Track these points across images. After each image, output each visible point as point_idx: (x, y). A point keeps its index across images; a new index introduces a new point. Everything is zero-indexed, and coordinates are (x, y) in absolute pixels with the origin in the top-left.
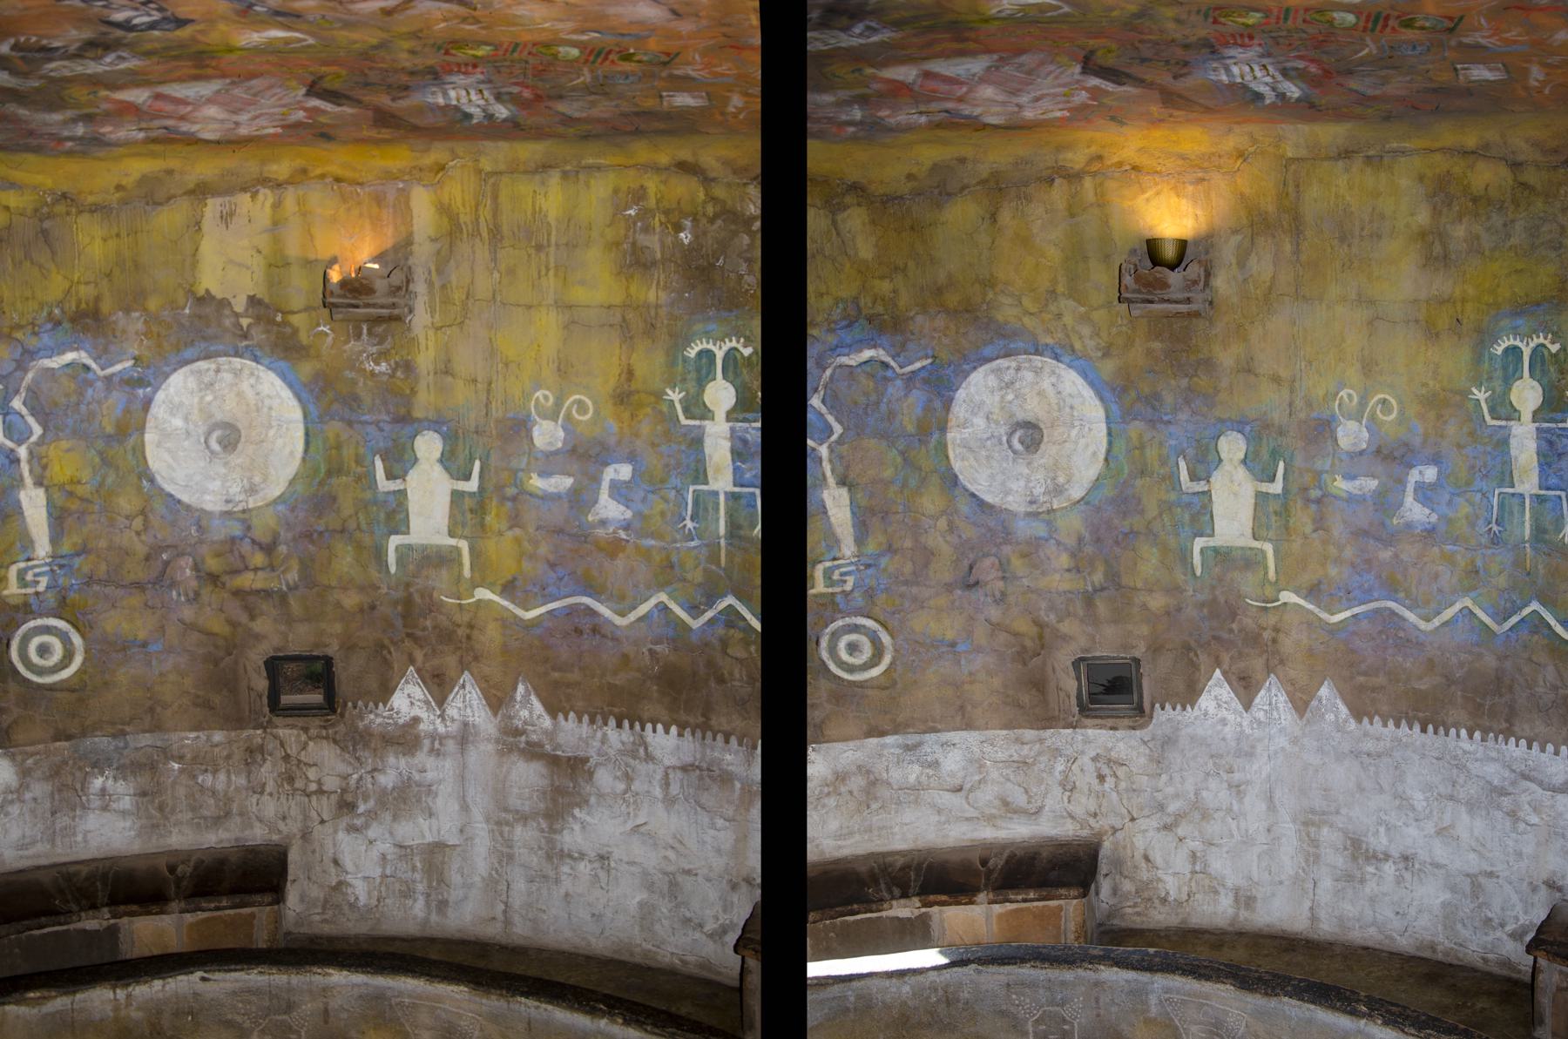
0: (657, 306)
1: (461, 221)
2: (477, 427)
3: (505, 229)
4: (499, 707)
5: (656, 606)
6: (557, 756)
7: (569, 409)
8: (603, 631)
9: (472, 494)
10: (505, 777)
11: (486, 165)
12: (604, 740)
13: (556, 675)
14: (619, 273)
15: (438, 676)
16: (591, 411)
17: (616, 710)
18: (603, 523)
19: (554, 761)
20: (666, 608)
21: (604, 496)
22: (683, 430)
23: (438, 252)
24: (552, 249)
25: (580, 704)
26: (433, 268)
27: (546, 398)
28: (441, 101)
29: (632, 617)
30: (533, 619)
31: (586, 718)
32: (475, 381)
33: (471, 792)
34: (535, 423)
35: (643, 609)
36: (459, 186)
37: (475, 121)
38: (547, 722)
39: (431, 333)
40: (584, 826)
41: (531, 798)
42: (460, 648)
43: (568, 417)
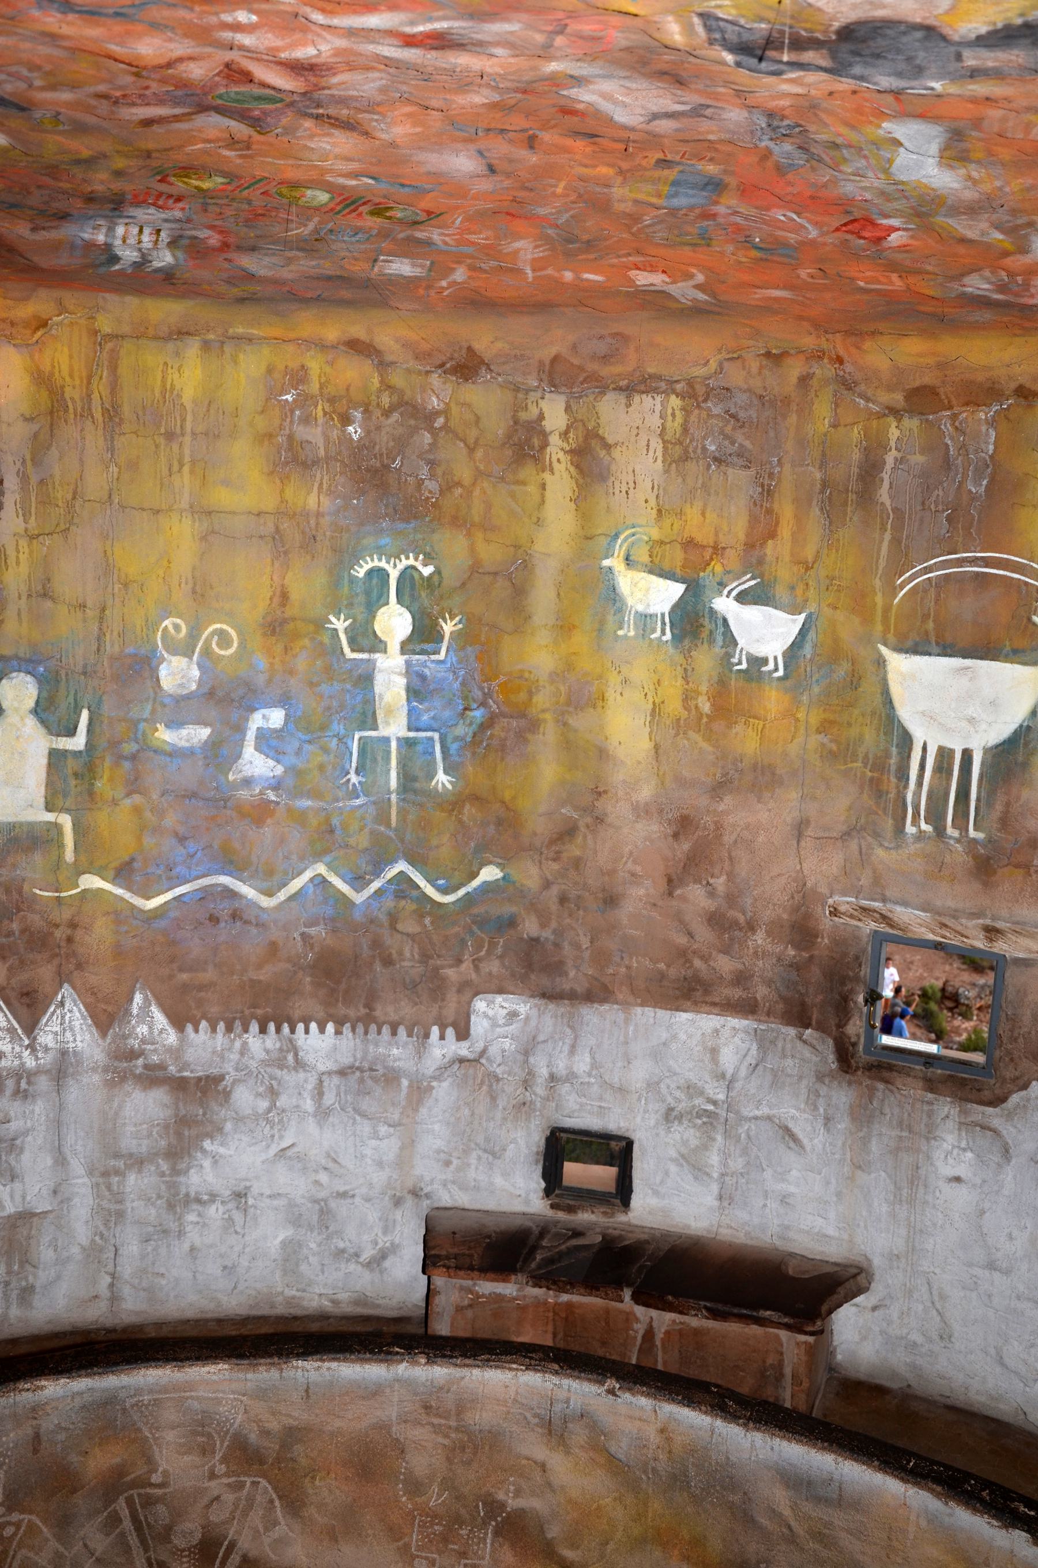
0: (319, 515)
1: (67, 396)
2: (85, 666)
3: (126, 410)
4: (110, 1025)
5: (312, 880)
6: (183, 1078)
7: (208, 641)
8: (245, 917)
9: (77, 754)
10: (116, 1114)
11: (105, 324)
12: (244, 1050)
13: (185, 976)
14: (271, 473)
15: (27, 994)
16: (235, 645)
17: (259, 1012)
18: (248, 782)
19: (180, 1085)
20: (324, 881)
21: (249, 751)
22: (348, 666)
23: (36, 436)
24: (187, 439)
25: (214, 1010)
26: (28, 457)
27: (177, 627)
28: (101, 238)
29: (282, 896)
30: (156, 909)
31: (221, 1026)
32: (83, 606)
33: (70, 1139)
34: (163, 659)
35: (296, 885)
36: (66, 350)
37: (117, 267)
38: (172, 1037)
39: (23, 543)
40: (216, 1160)
41: (150, 1135)
42: (57, 955)
43: (207, 652)
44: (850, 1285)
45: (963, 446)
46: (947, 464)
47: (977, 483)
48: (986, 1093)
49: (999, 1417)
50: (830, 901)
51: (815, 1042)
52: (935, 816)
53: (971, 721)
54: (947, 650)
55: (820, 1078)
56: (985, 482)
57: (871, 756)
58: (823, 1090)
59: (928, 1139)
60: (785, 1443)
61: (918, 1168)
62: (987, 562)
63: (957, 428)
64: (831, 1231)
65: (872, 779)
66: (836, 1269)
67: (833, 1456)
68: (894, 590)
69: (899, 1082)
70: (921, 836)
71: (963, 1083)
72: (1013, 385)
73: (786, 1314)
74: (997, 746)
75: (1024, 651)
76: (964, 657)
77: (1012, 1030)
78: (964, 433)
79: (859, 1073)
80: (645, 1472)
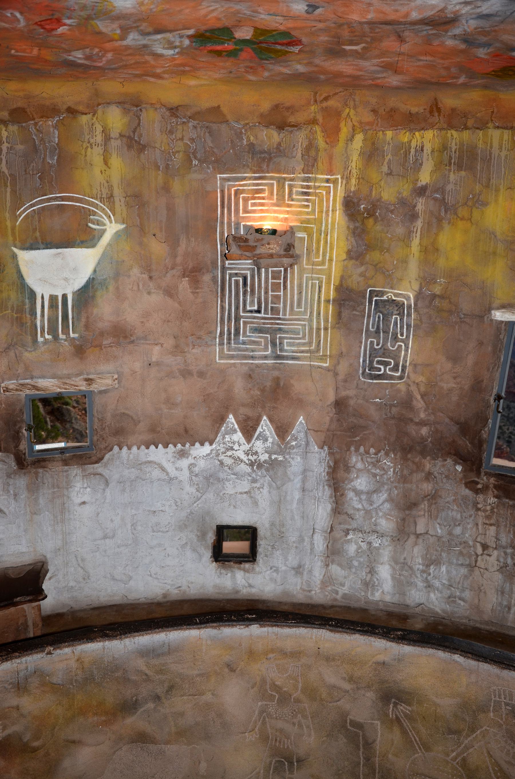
44: (43, 571)
45: (42, 140)
46: (35, 150)
47: (52, 158)
48: (93, 458)
49: (116, 603)
50: (3, 385)
51: (4, 459)
52: (53, 330)
53: (66, 279)
54: (48, 246)
55: (9, 476)
56: (56, 158)
57: (15, 306)
58: (11, 481)
59: (67, 489)
60: (141, 638)
61: (64, 504)
62: (63, 199)
63: (38, 130)
64: (24, 550)
65: (17, 318)
66: (31, 567)
67: (164, 633)
68: (16, 218)
69: (50, 465)
70: (46, 341)
71: (80, 457)
72: (65, 107)
73: (28, 595)
74: (79, 290)
75: (86, 241)
76: (57, 248)
77: (102, 425)
78: (42, 133)
79: (29, 467)
80: (72, 684)
